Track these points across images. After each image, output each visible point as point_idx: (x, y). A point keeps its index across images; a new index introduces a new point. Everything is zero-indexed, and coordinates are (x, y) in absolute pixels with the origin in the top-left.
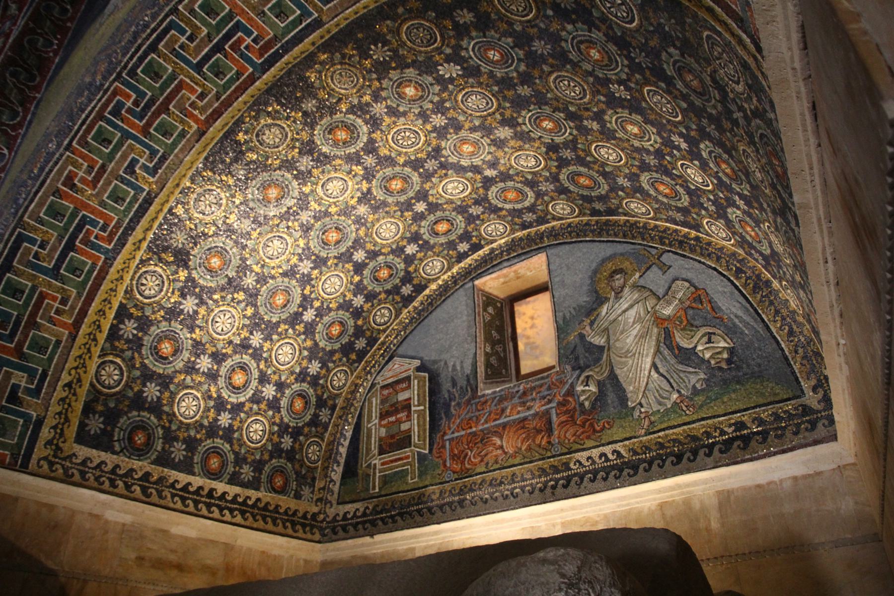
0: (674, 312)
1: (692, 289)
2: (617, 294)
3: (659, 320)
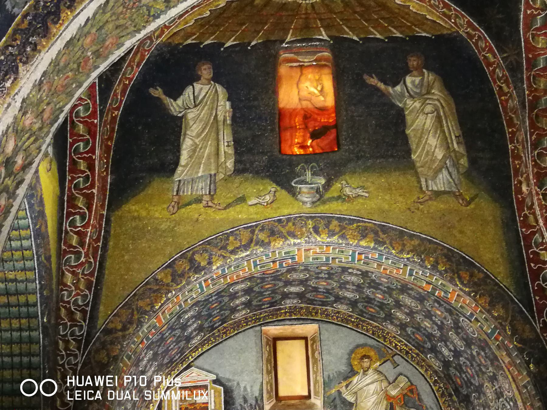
0: (398, 395)
1: (409, 383)
2: (365, 371)
3: (388, 397)
